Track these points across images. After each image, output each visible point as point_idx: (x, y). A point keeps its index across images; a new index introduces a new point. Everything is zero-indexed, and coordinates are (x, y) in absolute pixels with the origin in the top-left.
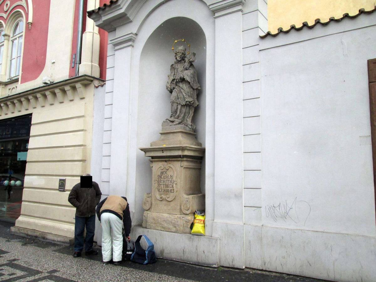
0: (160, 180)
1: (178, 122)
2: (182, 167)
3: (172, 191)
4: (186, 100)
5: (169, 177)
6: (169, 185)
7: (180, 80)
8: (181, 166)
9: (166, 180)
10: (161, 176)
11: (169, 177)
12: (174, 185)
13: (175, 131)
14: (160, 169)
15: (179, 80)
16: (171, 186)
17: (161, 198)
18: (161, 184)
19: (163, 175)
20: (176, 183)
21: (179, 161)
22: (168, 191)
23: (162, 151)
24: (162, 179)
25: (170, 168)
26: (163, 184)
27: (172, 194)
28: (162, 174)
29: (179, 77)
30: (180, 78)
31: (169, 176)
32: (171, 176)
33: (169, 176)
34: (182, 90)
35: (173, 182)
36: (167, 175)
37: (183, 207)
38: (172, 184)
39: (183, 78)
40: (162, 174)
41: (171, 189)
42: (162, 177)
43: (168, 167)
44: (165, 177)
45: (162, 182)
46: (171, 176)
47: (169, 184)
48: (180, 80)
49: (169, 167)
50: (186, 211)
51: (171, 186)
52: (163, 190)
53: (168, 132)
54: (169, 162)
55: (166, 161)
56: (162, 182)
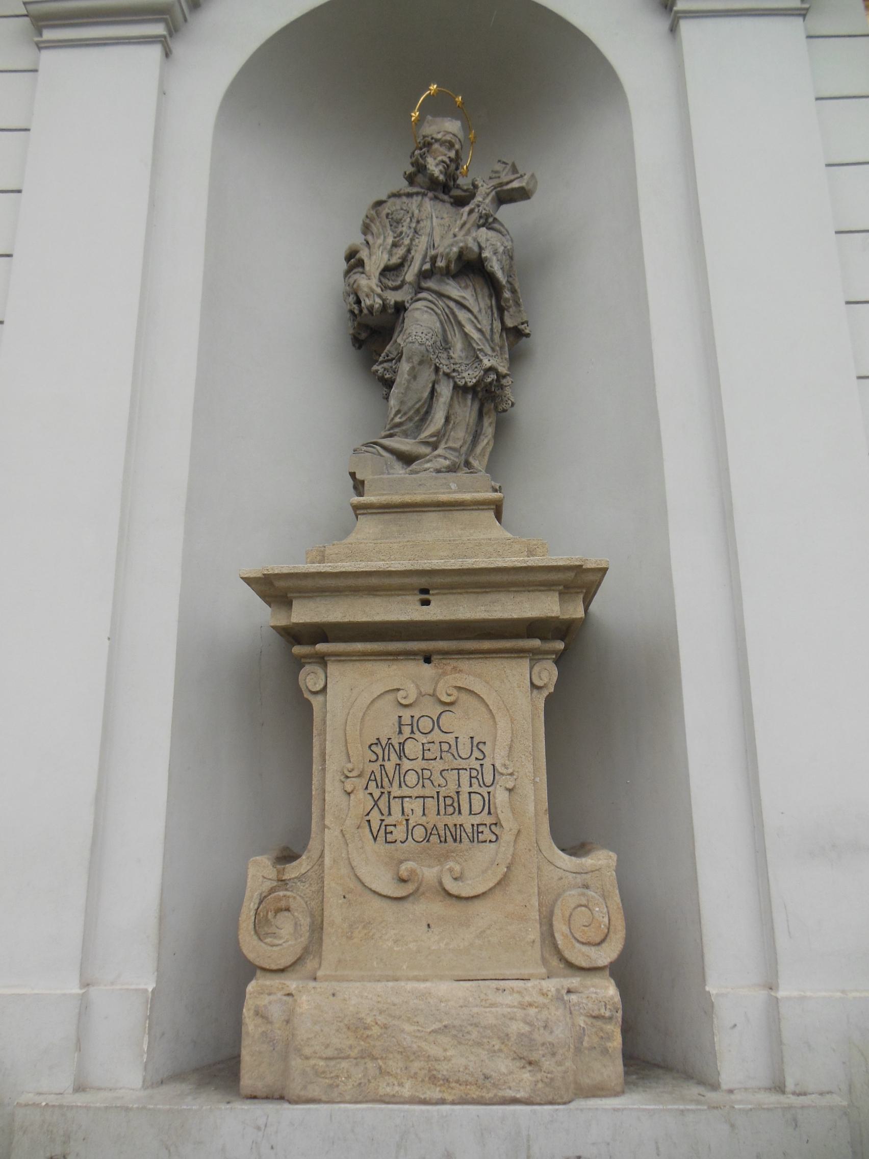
0: (390, 766)
1: (447, 462)
2: (539, 688)
3: (487, 835)
4: (487, 363)
5: (464, 751)
6: (464, 798)
7: (452, 266)
8: (533, 685)
9: (438, 766)
10: (402, 744)
11: (464, 751)
12: (501, 797)
13: (467, 497)
14: (390, 697)
15: (449, 263)
16: (477, 801)
17: (403, 881)
18: (406, 791)
19: (418, 735)
20: (510, 785)
21: (519, 653)
22: (455, 835)
23: (425, 591)
24: (407, 765)
25: (464, 696)
26: (418, 791)
27: (484, 854)
28: (407, 730)
29: (455, 249)
30: (460, 254)
31: (464, 741)
32: (477, 745)
33: (464, 741)
34: (462, 315)
35: (488, 779)
36: (450, 738)
37: (565, 929)
38: (484, 791)
39: (473, 256)
40: (407, 730)
41: (476, 820)
42: (411, 748)
43: (455, 692)
44: (435, 748)
45: (411, 778)
46: (477, 745)
47: (465, 789)
48: (452, 266)
49: (459, 689)
50: (585, 949)
51: (477, 808)
52: (419, 833)
53: (418, 498)
54: (453, 663)
55: (428, 660)
56: (411, 778)
